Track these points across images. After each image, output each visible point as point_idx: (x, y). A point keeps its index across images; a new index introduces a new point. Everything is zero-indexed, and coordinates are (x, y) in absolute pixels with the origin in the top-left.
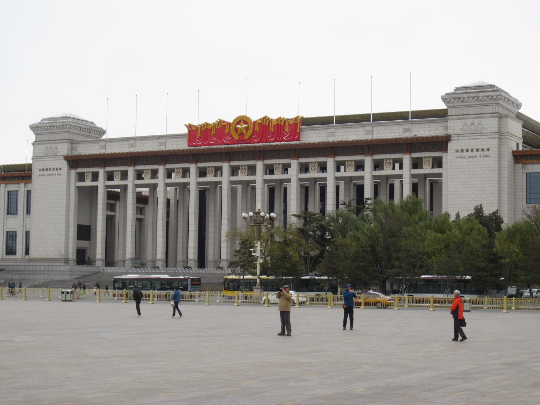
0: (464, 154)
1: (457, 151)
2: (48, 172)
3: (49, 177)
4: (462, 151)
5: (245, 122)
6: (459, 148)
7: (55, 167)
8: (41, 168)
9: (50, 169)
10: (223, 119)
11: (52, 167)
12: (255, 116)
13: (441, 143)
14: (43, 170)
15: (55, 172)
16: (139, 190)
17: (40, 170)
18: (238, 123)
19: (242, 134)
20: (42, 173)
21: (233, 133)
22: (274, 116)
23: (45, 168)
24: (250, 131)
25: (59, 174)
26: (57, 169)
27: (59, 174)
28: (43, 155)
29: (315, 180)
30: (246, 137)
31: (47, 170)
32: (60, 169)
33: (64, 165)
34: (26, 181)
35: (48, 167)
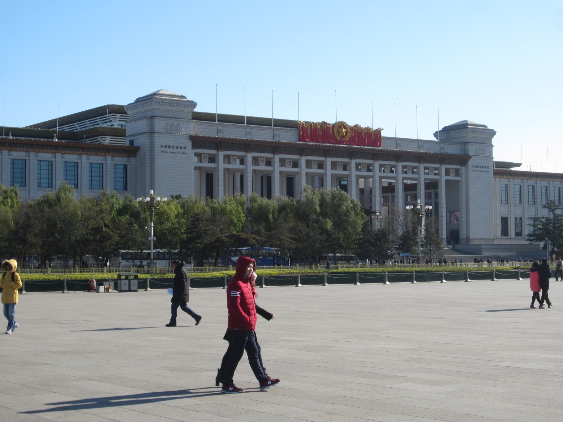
0: (477, 169)
1: (473, 166)
2: (171, 150)
3: (172, 155)
4: (476, 167)
5: (345, 128)
6: (474, 165)
7: (179, 145)
8: (164, 144)
9: (173, 147)
10: (326, 121)
11: (175, 145)
12: (351, 123)
13: (463, 160)
14: (166, 147)
15: (179, 150)
16: (405, 181)
17: (162, 147)
18: (340, 127)
19: (342, 137)
20: (163, 149)
21: (336, 135)
22: (363, 125)
23: (168, 145)
24: (349, 135)
25: (183, 153)
26: (181, 148)
27: (183, 153)
28: (164, 131)
29: (238, 170)
30: (347, 139)
31: (170, 147)
32: (185, 148)
33: (190, 143)
34: (63, 152)
35: (171, 145)
